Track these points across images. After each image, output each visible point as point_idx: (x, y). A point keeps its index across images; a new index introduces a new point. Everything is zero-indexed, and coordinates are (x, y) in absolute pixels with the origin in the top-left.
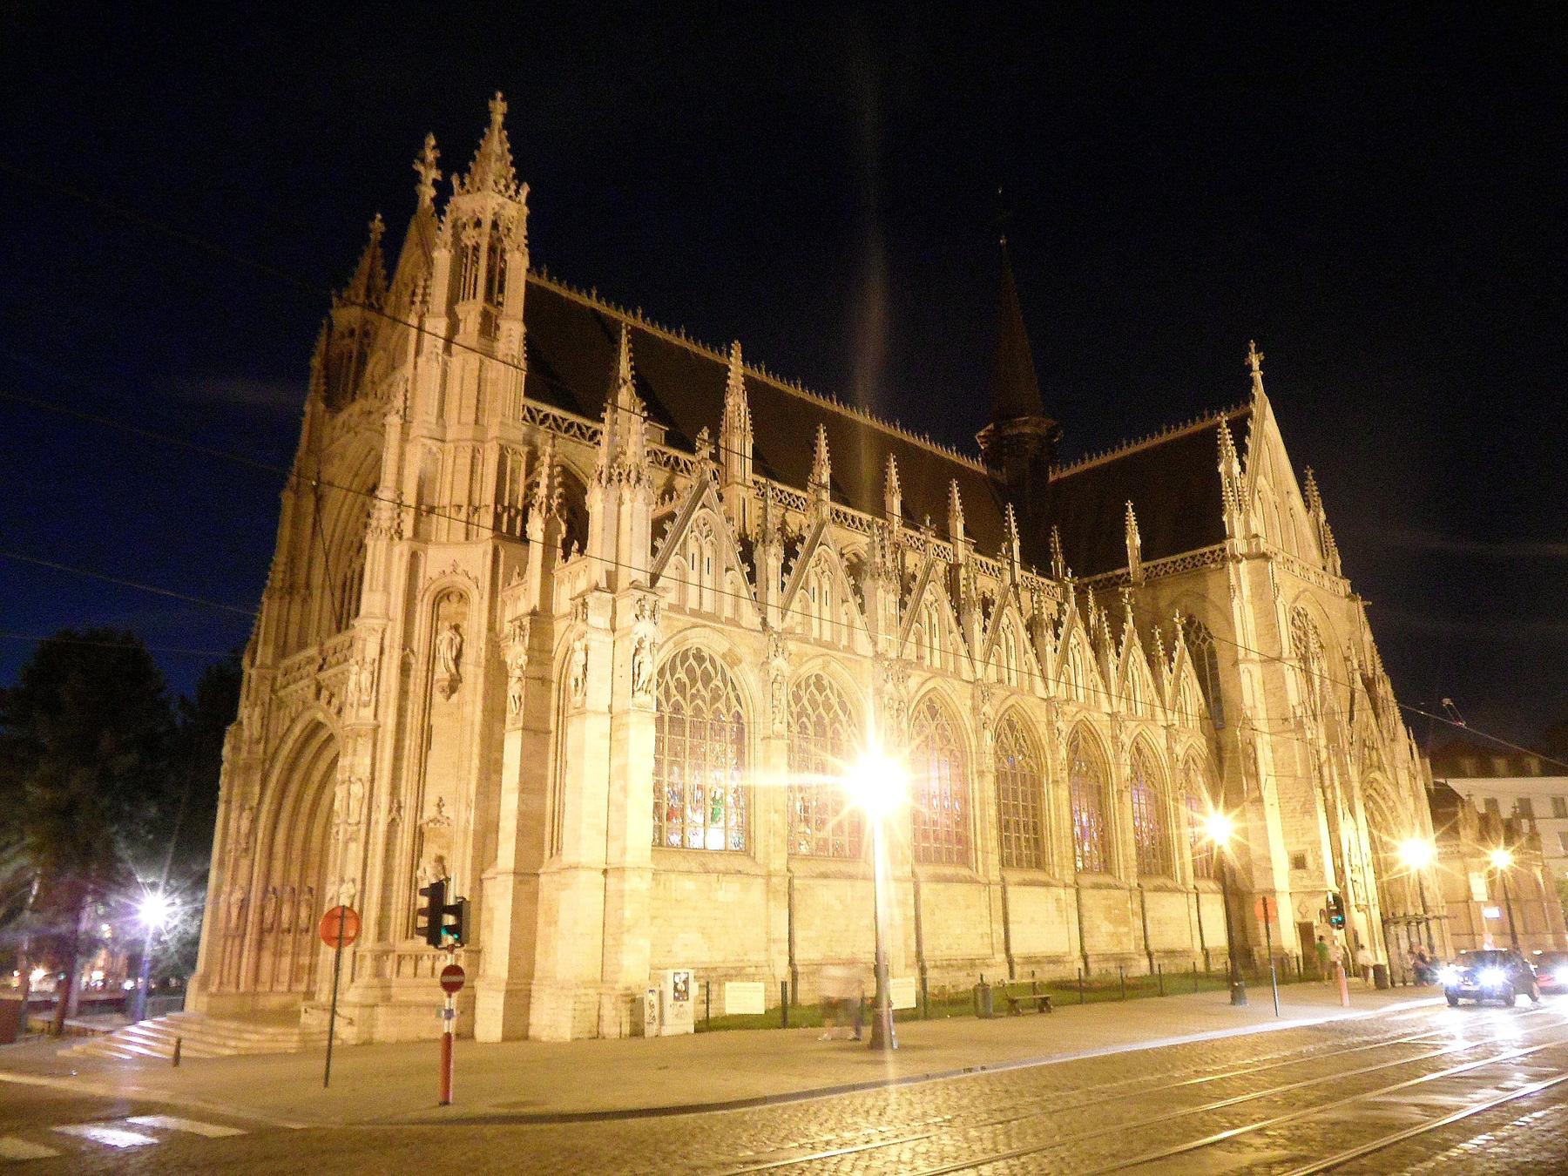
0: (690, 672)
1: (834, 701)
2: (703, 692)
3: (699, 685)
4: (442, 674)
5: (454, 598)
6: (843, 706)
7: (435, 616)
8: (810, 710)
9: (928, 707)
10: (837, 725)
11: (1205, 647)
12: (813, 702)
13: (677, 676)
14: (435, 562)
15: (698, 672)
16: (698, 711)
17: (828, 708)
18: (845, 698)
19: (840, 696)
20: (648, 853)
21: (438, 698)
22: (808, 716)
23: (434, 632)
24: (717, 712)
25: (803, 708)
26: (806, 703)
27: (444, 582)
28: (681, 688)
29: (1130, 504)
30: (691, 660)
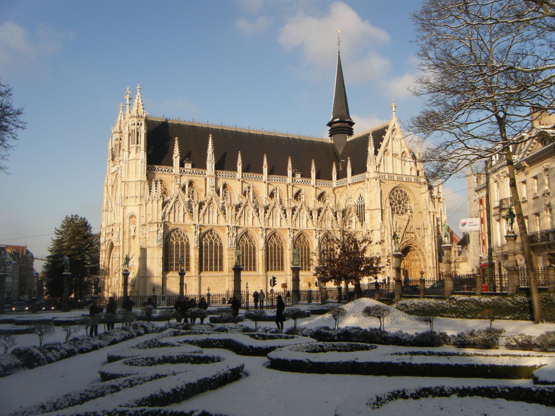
1: (216, 236)
4: (132, 234)
5: (134, 217)
6: (218, 237)
8: (208, 239)
12: (209, 237)
16: (177, 243)
17: (213, 237)
20: (161, 273)
21: (132, 239)
22: (208, 241)
24: (182, 243)
25: (206, 239)
27: (131, 214)
29: (349, 158)
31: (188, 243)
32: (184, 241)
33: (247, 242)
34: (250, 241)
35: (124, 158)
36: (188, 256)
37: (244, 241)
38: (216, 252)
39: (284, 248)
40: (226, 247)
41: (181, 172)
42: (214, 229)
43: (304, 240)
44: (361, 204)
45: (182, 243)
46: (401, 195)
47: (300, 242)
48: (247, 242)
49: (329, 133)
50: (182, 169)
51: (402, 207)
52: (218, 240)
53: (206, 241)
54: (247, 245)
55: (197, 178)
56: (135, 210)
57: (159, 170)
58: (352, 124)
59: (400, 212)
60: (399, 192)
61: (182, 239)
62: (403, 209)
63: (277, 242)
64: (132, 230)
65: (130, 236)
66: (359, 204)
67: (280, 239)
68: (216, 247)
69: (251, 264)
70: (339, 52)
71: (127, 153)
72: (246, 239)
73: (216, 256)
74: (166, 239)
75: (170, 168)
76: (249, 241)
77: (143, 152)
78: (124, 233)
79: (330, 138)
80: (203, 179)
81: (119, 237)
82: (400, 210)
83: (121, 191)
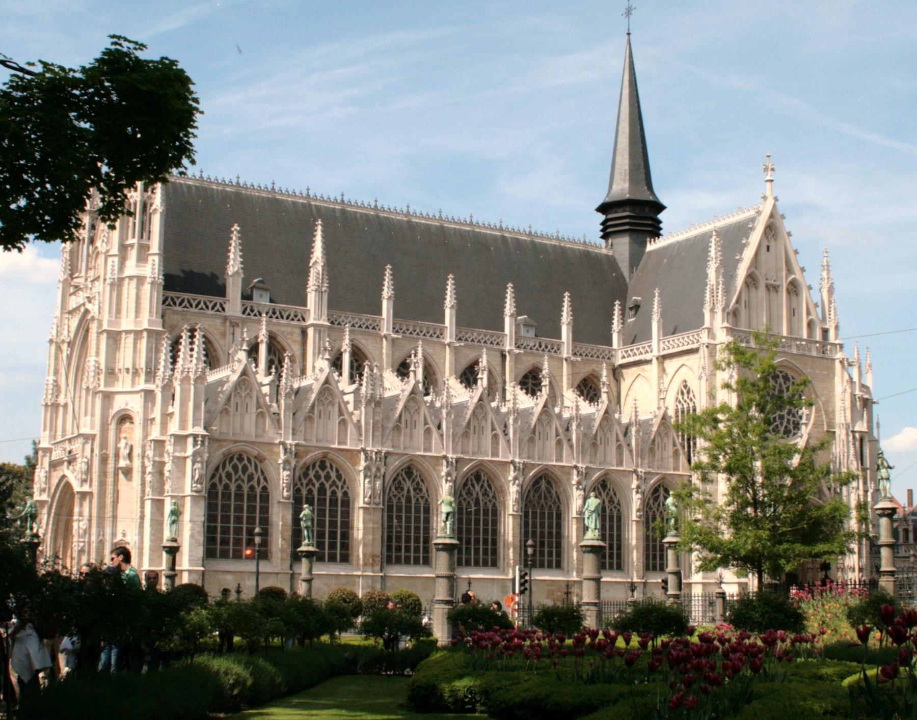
0: (235, 468)
1: (333, 475)
2: (242, 476)
3: (240, 473)
6: (339, 477)
7: (118, 431)
8: (315, 481)
9: (406, 473)
10: (334, 488)
11: (691, 405)
12: (318, 477)
13: (226, 470)
14: (119, 403)
15: (240, 467)
16: (239, 487)
17: (328, 477)
18: (341, 472)
19: (337, 471)
22: (314, 485)
23: (118, 439)
24: (252, 488)
25: (311, 480)
26: (313, 478)
28: (229, 476)
29: (657, 292)
30: (235, 461)
31: (265, 489)
32: (256, 485)
33: (409, 491)
34: (418, 489)
35: (109, 271)
36: (265, 521)
37: (402, 489)
38: (333, 514)
39: (500, 508)
40: (360, 502)
41: (244, 313)
42: (330, 456)
43: (550, 492)
44: (685, 406)
45: (252, 488)
46: (784, 387)
47: (540, 497)
48: (409, 491)
49: (602, 231)
50: (249, 303)
51: (786, 416)
52: (340, 484)
53: (310, 486)
54: (408, 500)
55: (284, 329)
56: (135, 405)
57: (191, 305)
58: (660, 208)
59: (782, 429)
60: (781, 380)
61: (251, 478)
62: (788, 421)
63: (483, 495)
64: (124, 452)
65: (117, 470)
66: (680, 407)
67: (490, 486)
68: (334, 502)
69: (419, 547)
70: (629, 34)
71: (116, 259)
72: (408, 484)
73: (333, 524)
74: (213, 476)
75: (219, 300)
76: (415, 490)
77: (156, 258)
78: (104, 460)
79: (603, 242)
80: (298, 331)
81: (89, 471)
82: (781, 423)
83: (98, 354)
